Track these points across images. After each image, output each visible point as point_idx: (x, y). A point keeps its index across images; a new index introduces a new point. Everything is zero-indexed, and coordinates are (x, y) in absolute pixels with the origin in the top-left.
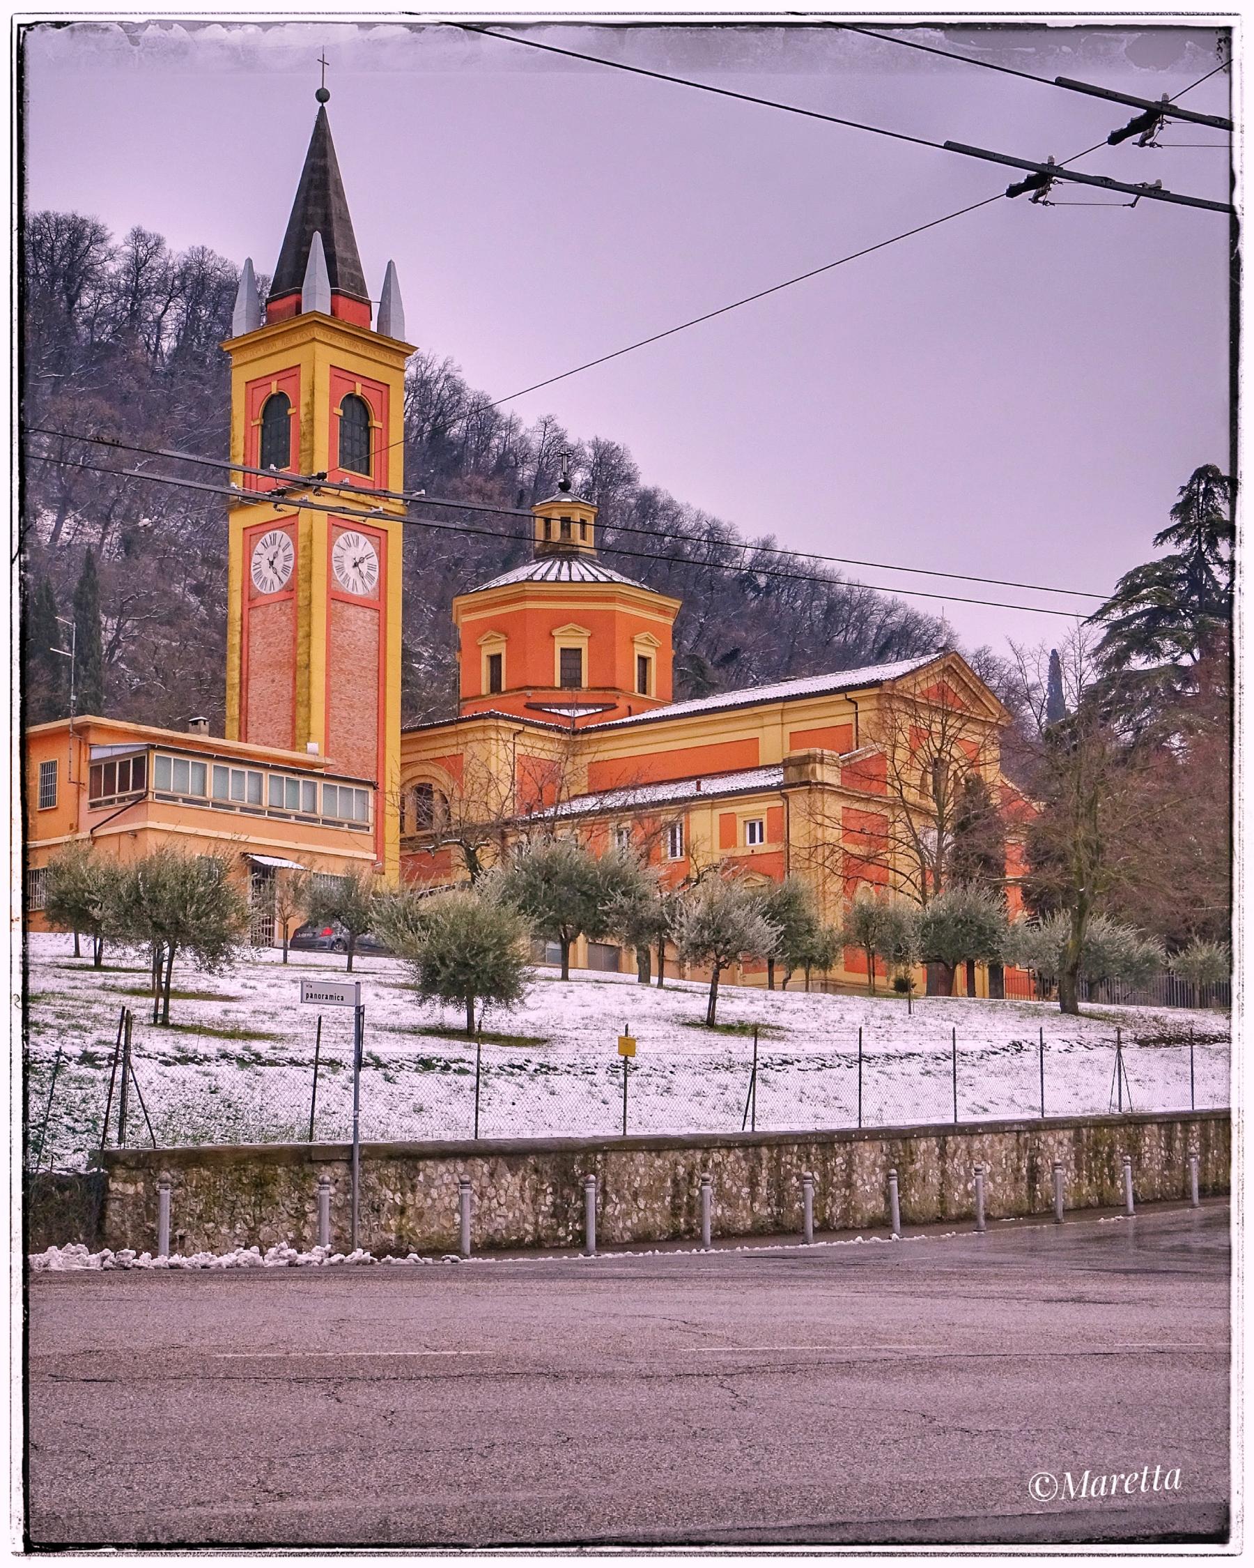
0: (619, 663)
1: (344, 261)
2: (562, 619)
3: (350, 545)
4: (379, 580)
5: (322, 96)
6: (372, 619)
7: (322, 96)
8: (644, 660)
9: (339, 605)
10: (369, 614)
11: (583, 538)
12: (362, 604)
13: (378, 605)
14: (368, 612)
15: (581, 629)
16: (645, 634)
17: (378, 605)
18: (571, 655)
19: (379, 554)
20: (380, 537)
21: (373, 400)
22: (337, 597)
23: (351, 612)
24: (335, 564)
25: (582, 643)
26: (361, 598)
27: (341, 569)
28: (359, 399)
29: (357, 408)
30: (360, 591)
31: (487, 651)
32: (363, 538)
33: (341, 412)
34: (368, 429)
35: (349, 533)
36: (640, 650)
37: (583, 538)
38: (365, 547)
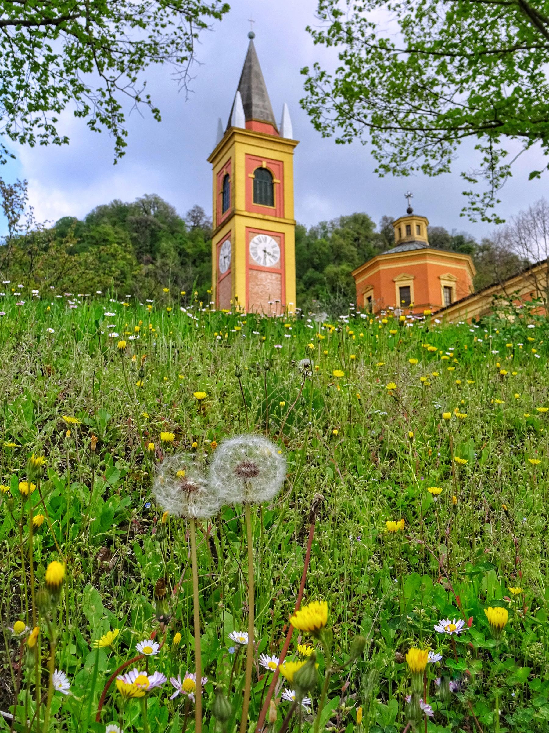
0: (431, 290)
1: (257, 106)
2: (398, 271)
3: (260, 242)
4: (281, 259)
5: (251, 37)
6: (277, 278)
7: (251, 37)
8: (449, 288)
9: (255, 272)
10: (274, 276)
11: (419, 233)
12: (271, 271)
13: (281, 271)
14: (274, 275)
15: (406, 275)
16: (447, 274)
17: (281, 271)
18: (405, 290)
19: (280, 245)
20: (280, 236)
21: (274, 169)
22: (251, 268)
23: (263, 275)
24: (251, 252)
25: (409, 283)
26: (269, 268)
27: (255, 254)
28: (266, 170)
29: (265, 173)
30: (268, 265)
31: (367, 295)
32: (269, 238)
33: (253, 176)
34: (272, 184)
35: (261, 236)
36: (444, 283)
37: (419, 233)
38: (270, 243)
